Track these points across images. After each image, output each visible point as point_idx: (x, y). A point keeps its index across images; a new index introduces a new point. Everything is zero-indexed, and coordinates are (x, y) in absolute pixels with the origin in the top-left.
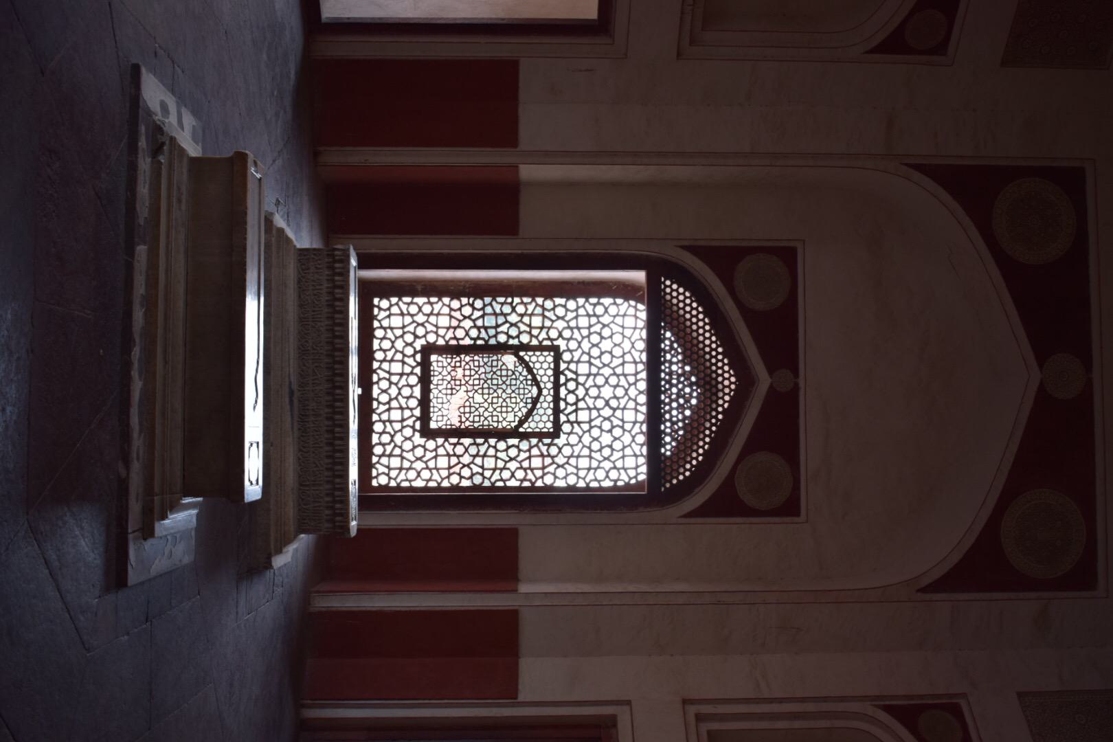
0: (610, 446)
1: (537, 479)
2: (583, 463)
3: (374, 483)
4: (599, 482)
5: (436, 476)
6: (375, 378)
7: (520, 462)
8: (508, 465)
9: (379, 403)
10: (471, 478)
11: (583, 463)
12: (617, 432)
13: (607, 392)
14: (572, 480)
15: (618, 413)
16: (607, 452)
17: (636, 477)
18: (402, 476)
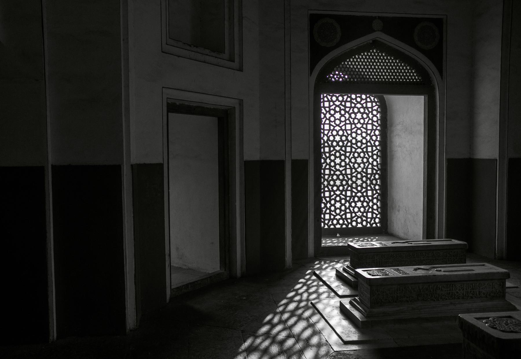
0: (362, 114)
1: (377, 149)
2: (370, 127)
3: (378, 225)
4: (378, 120)
5: (375, 196)
6: (332, 227)
7: (369, 157)
8: (371, 162)
9: (344, 224)
10: (376, 180)
11: (370, 127)
12: (356, 110)
13: (337, 116)
14: (377, 133)
15: (347, 109)
16: (365, 116)
17: (376, 102)
18: (376, 212)
